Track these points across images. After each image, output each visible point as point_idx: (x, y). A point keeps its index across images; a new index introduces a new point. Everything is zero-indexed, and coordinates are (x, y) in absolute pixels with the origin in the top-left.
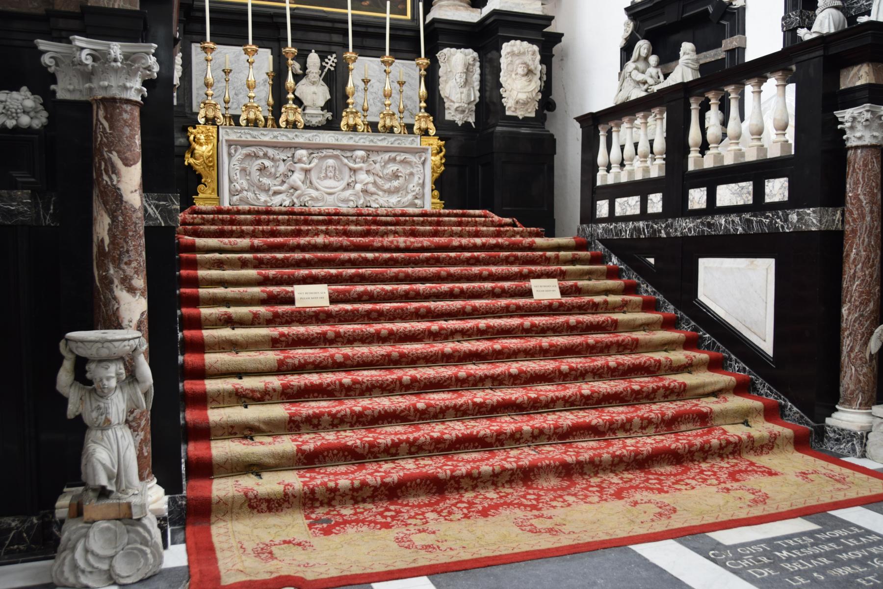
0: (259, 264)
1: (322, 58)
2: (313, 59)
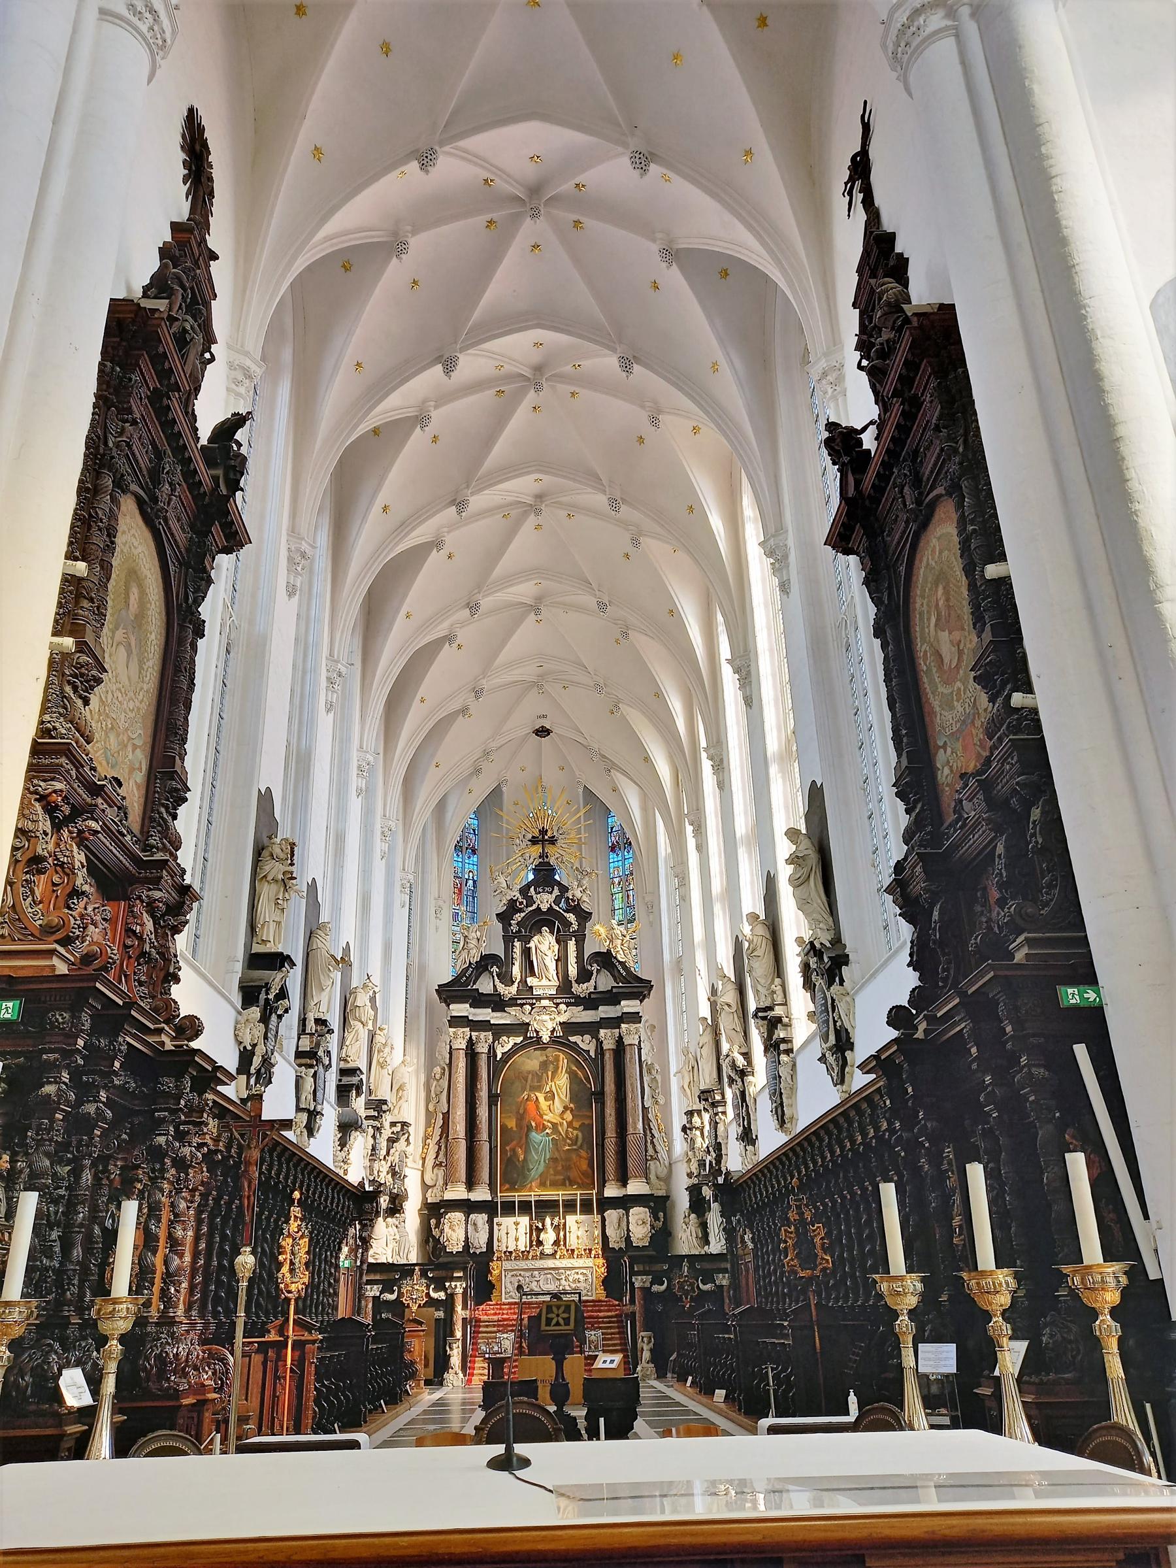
0: (499, 1326)
1: (552, 1220)
2: (548, 1220)
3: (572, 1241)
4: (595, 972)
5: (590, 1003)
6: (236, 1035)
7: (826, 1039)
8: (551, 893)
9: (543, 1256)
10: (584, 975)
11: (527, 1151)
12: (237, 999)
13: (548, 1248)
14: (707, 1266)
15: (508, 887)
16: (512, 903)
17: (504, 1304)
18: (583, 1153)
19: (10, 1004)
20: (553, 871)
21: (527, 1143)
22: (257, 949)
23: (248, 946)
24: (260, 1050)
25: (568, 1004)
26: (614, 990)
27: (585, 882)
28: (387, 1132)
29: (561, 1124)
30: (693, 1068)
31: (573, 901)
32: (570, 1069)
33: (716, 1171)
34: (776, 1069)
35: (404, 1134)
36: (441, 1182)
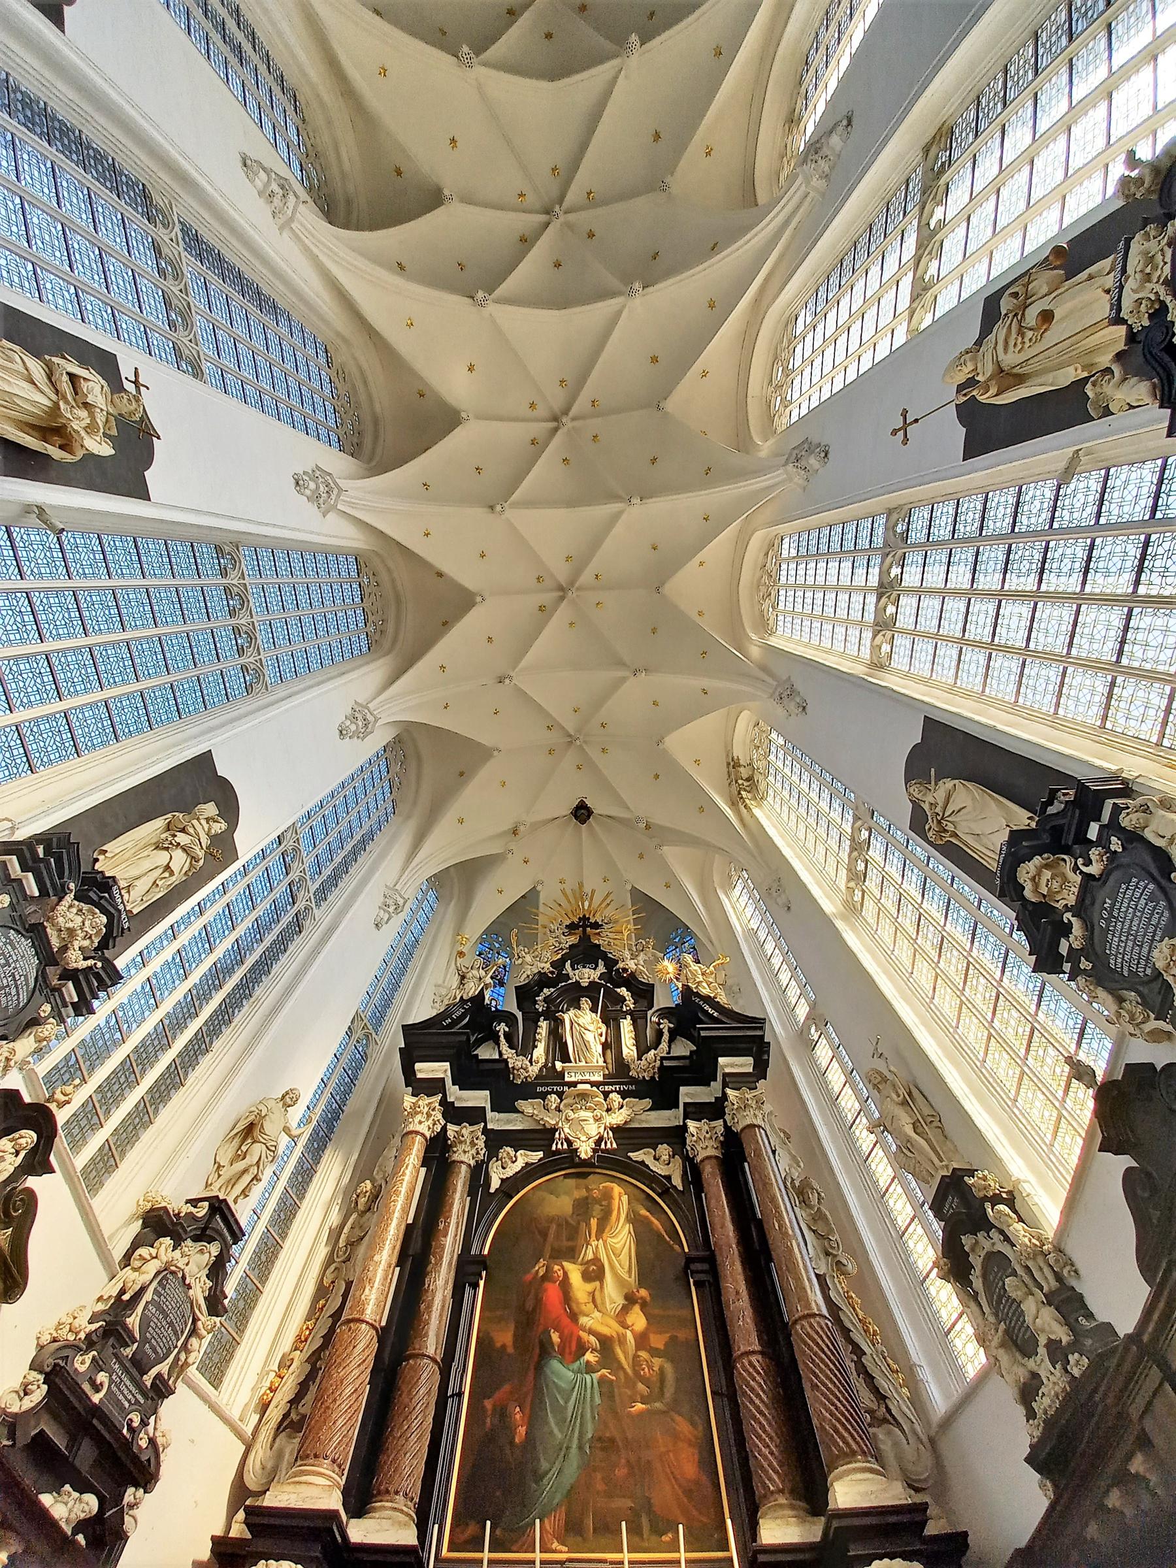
4: (666, 1031)
8: (595, 969)
11: (535, 1419)
21: (538, 1391)
29: (622, 1340)
30: (910, 1094)
32: (636, 1213)
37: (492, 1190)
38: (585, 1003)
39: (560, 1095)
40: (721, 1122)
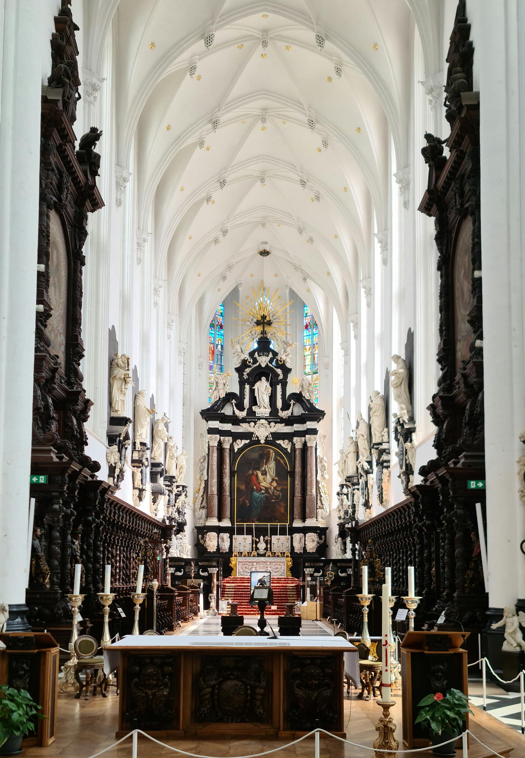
0: (235, 589)
1: (264, 537)
2: (262, 538)
3: (275, 548)
4: (292, 405)
5: (289, 421)
6: (107, 459)
7: (401, 468)
8: (268, 356)
9: (259, 555)
10: (286, 406)
12: (105, 440)
13: (262, 551)
14: (344, 565)
15: (242, 352)
16: (244, 362)
17: (238, 578)
18: (282, 504)
19: (43, 477)
20: (269, 343)
22: (114, 415)
23: (109, 413)
24: (119, 465)
25: (276, 423)
26: (303, 416)
27: (288, 350)
28: (175, 491)
29: (270, 488)
30: (345, 461)
31: (281, 361)
33: (353, 518)
34: (381, 475)
35: (184, 492)
36: (204, 516)
37: (235, 452)
38: (264, 379)
39: (255, 422)
40: (304, 438)
